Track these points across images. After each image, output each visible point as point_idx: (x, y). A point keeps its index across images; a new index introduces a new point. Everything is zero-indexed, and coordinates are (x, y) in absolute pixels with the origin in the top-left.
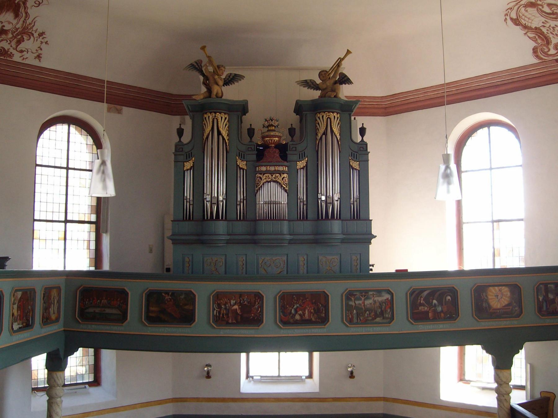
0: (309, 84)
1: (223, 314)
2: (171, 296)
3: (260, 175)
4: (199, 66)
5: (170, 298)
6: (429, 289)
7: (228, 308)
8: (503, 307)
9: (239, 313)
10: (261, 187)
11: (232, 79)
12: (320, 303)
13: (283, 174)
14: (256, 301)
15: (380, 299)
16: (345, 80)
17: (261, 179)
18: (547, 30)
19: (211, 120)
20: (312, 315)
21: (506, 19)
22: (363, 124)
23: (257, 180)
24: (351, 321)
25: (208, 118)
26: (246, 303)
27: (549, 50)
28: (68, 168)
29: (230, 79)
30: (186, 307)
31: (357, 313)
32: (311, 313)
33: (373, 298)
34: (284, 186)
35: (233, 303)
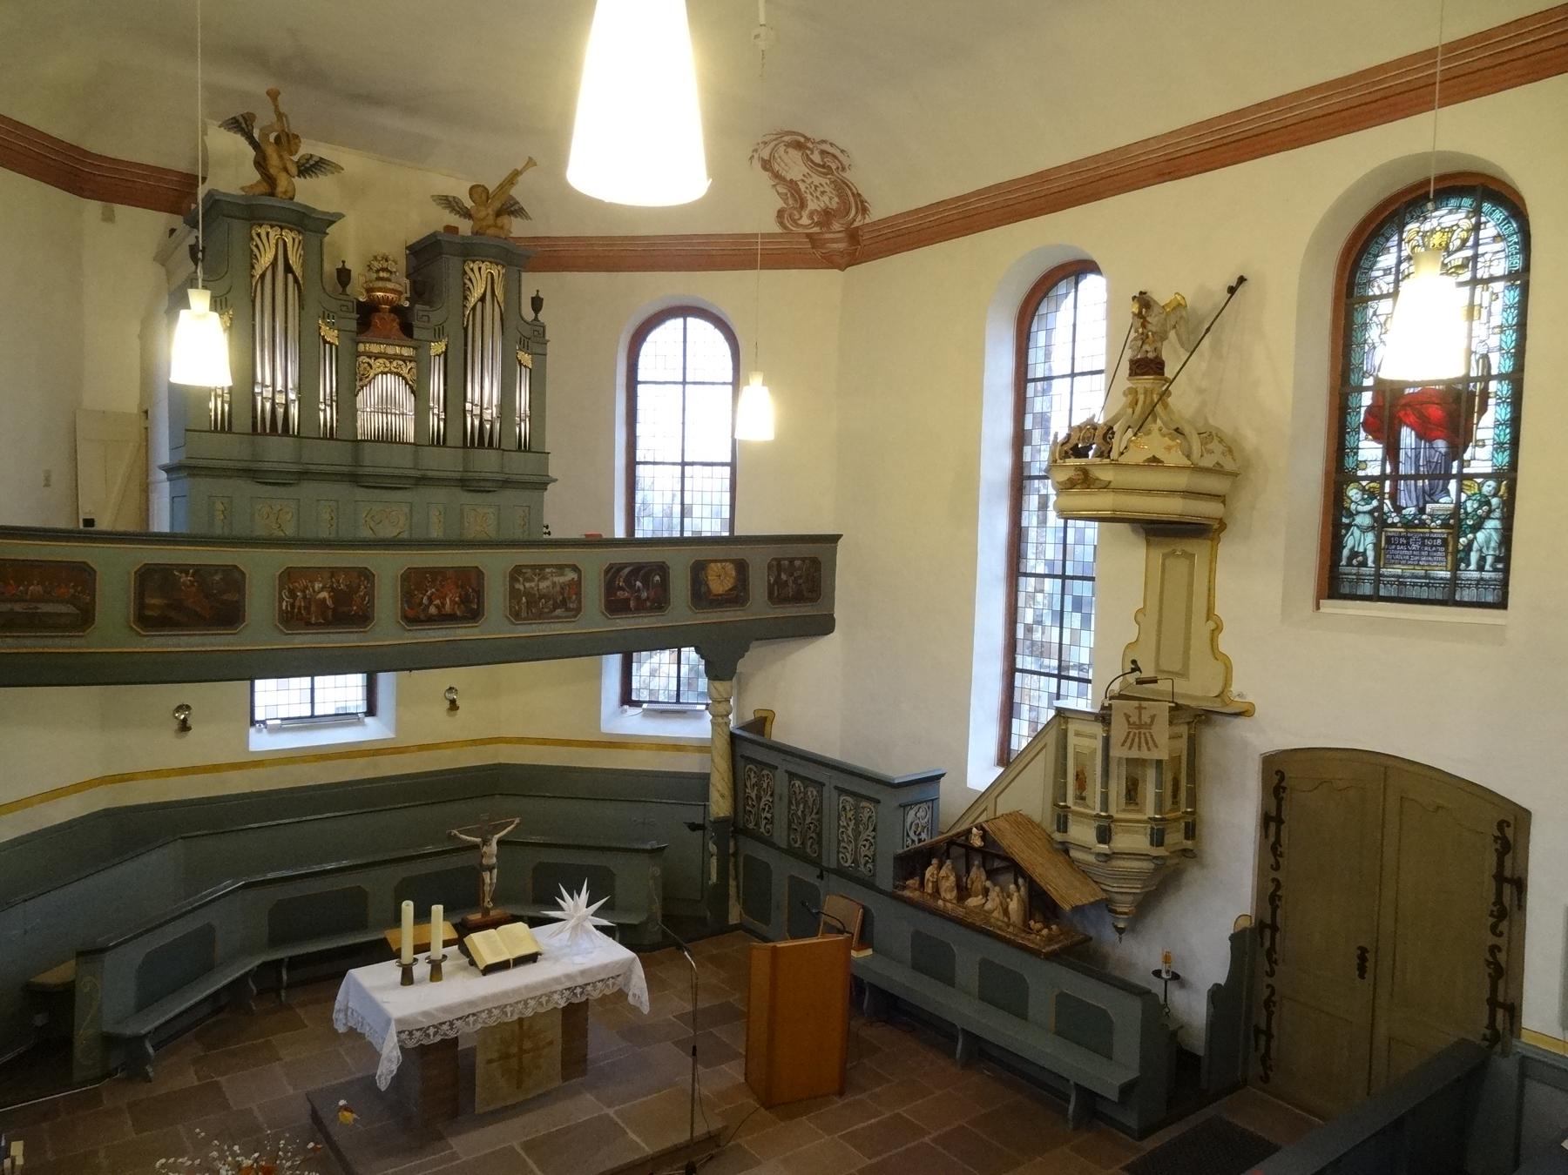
0: (450, 203)
1: (300, 608)
2: (192, 576)
3: (368, 360)
4: (247, 126)
5: (192, 579)
6: (630, 564)
8: (726, 591)
10: (370, 382)
11: (312, 166)
12: (470, 587)
13: (410, 361)
15: (562, 579)
16: (511, 209)
17: (371, 367)
18: (807, 188)
19: (273, 241)
20: (456, 606)
21: (753, 156)
22: (538, 291)
23: (362, 369)
24: (517, 615)
25: (266, 238)
27: (801, 217)
28: (684, 383)
29: (308, 165)
30: (225, 597)
31: (527, 602)
32: (454, 600)
33: (551, 578)
34: (410, 383)
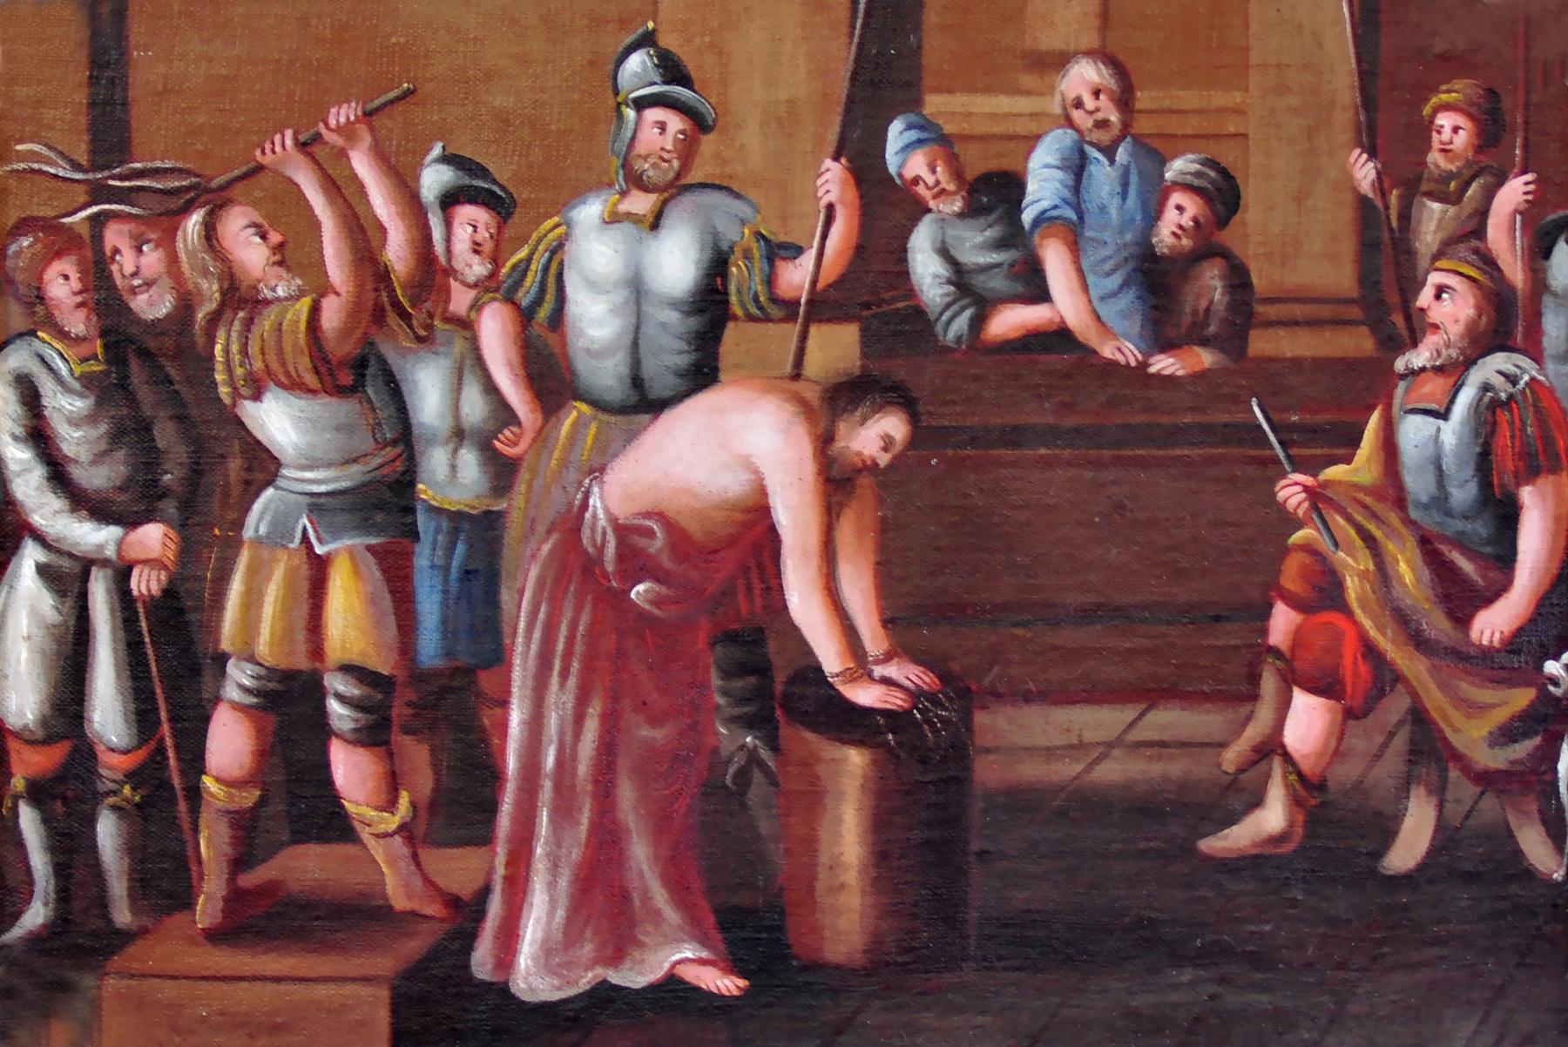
9: (830, 656)
14: (1433, 219)
35: (636, 288)
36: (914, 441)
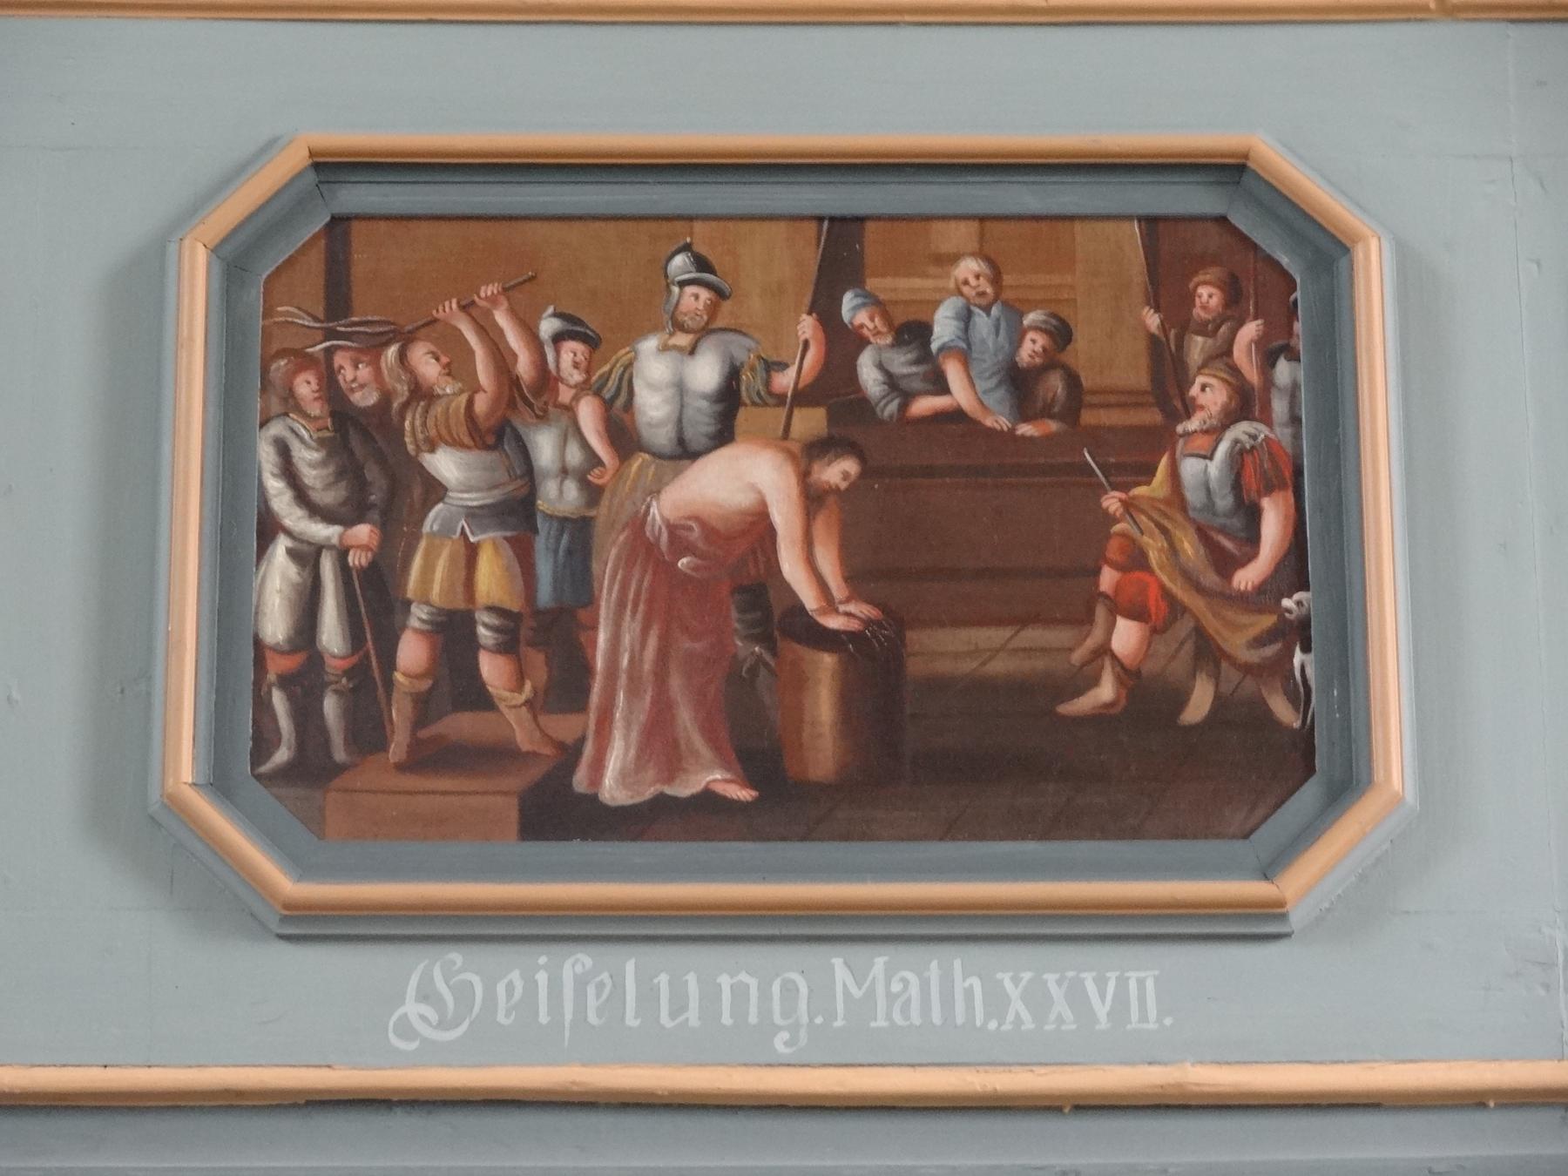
7: (561, 497)
9: (809, 598)
14: (1198, 347)
26: (960, 393)
35: (680, 388)
36: (863, 474)
